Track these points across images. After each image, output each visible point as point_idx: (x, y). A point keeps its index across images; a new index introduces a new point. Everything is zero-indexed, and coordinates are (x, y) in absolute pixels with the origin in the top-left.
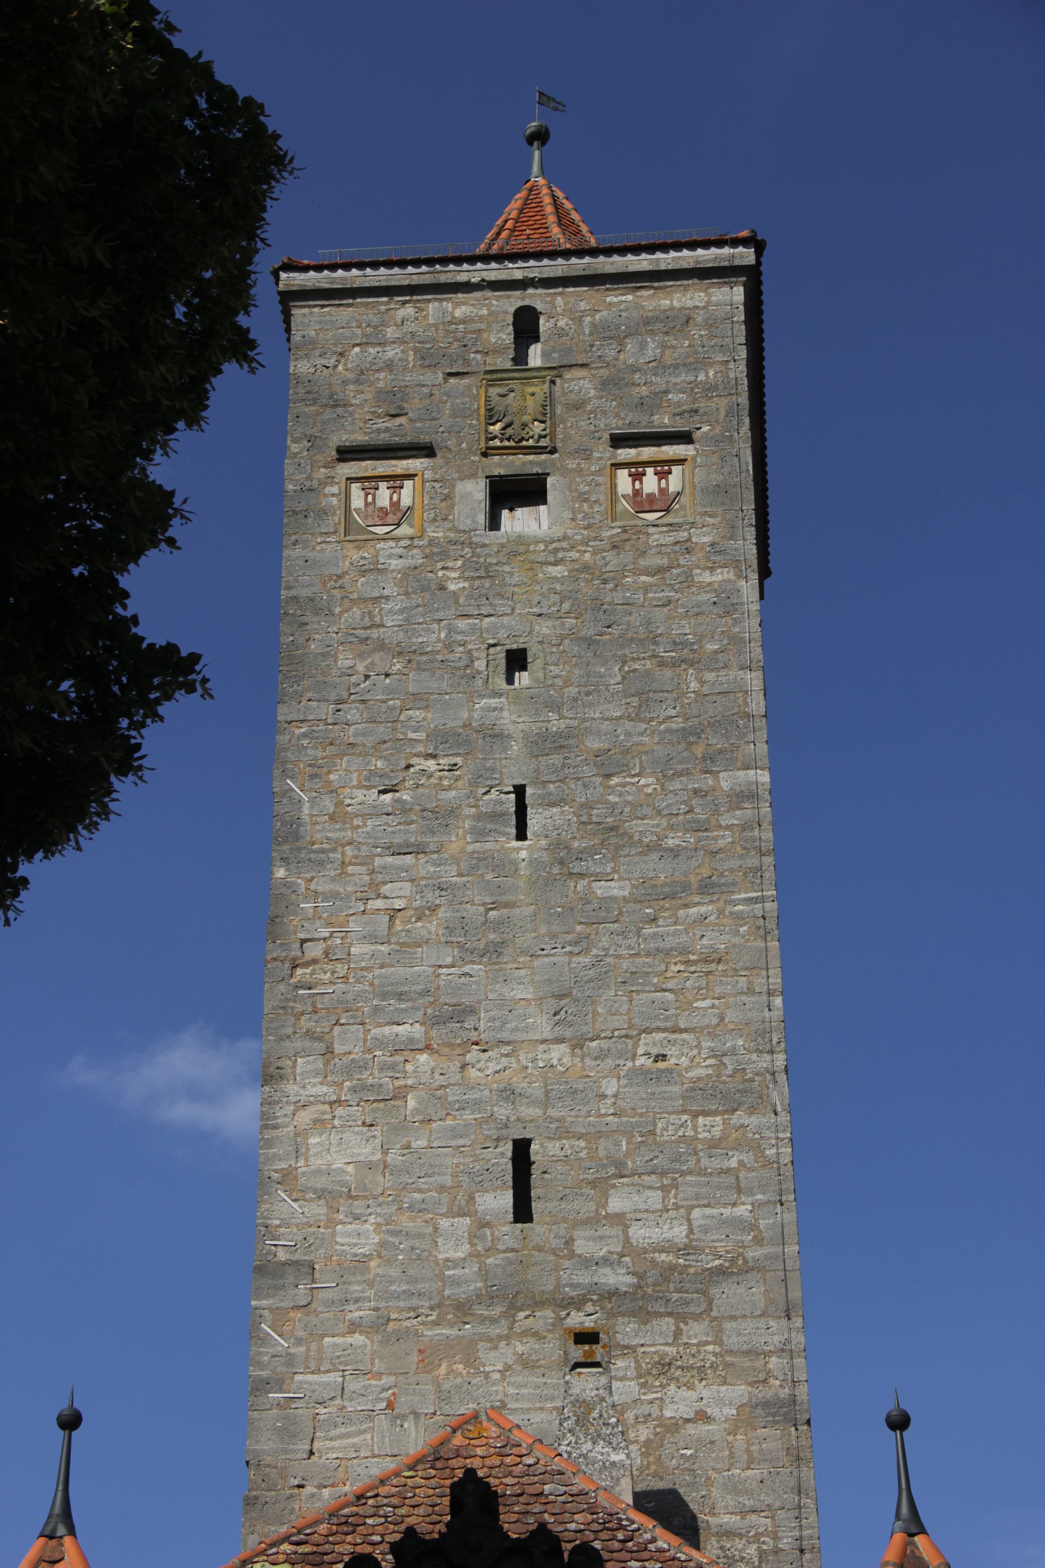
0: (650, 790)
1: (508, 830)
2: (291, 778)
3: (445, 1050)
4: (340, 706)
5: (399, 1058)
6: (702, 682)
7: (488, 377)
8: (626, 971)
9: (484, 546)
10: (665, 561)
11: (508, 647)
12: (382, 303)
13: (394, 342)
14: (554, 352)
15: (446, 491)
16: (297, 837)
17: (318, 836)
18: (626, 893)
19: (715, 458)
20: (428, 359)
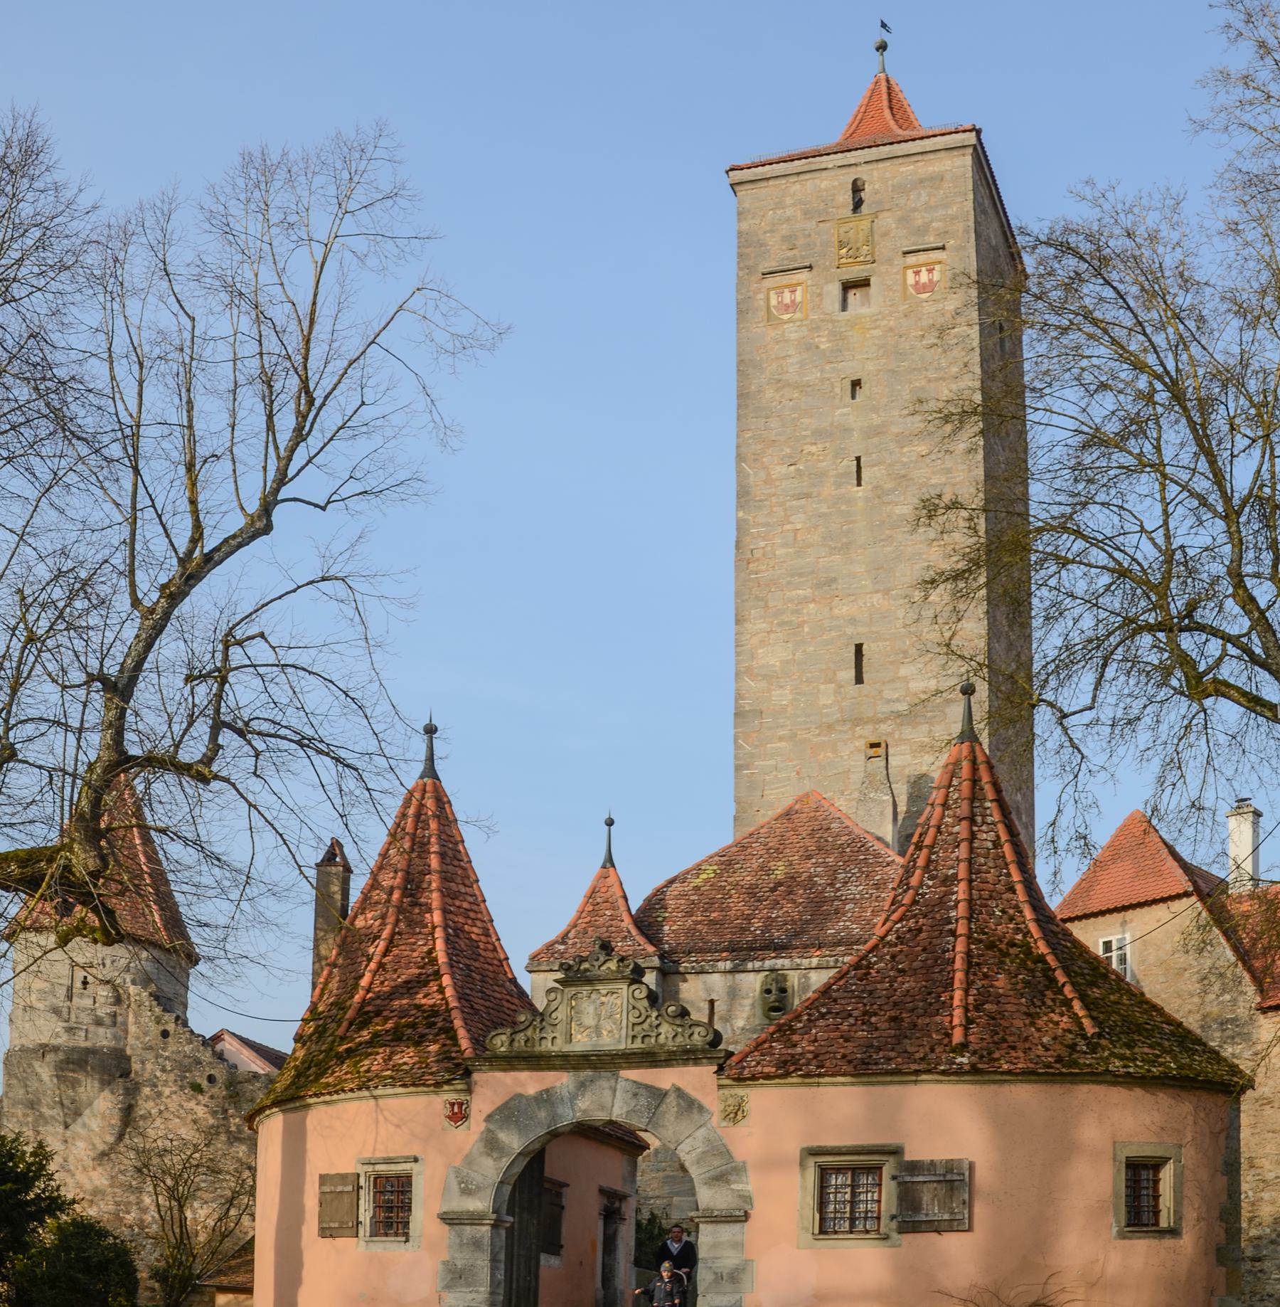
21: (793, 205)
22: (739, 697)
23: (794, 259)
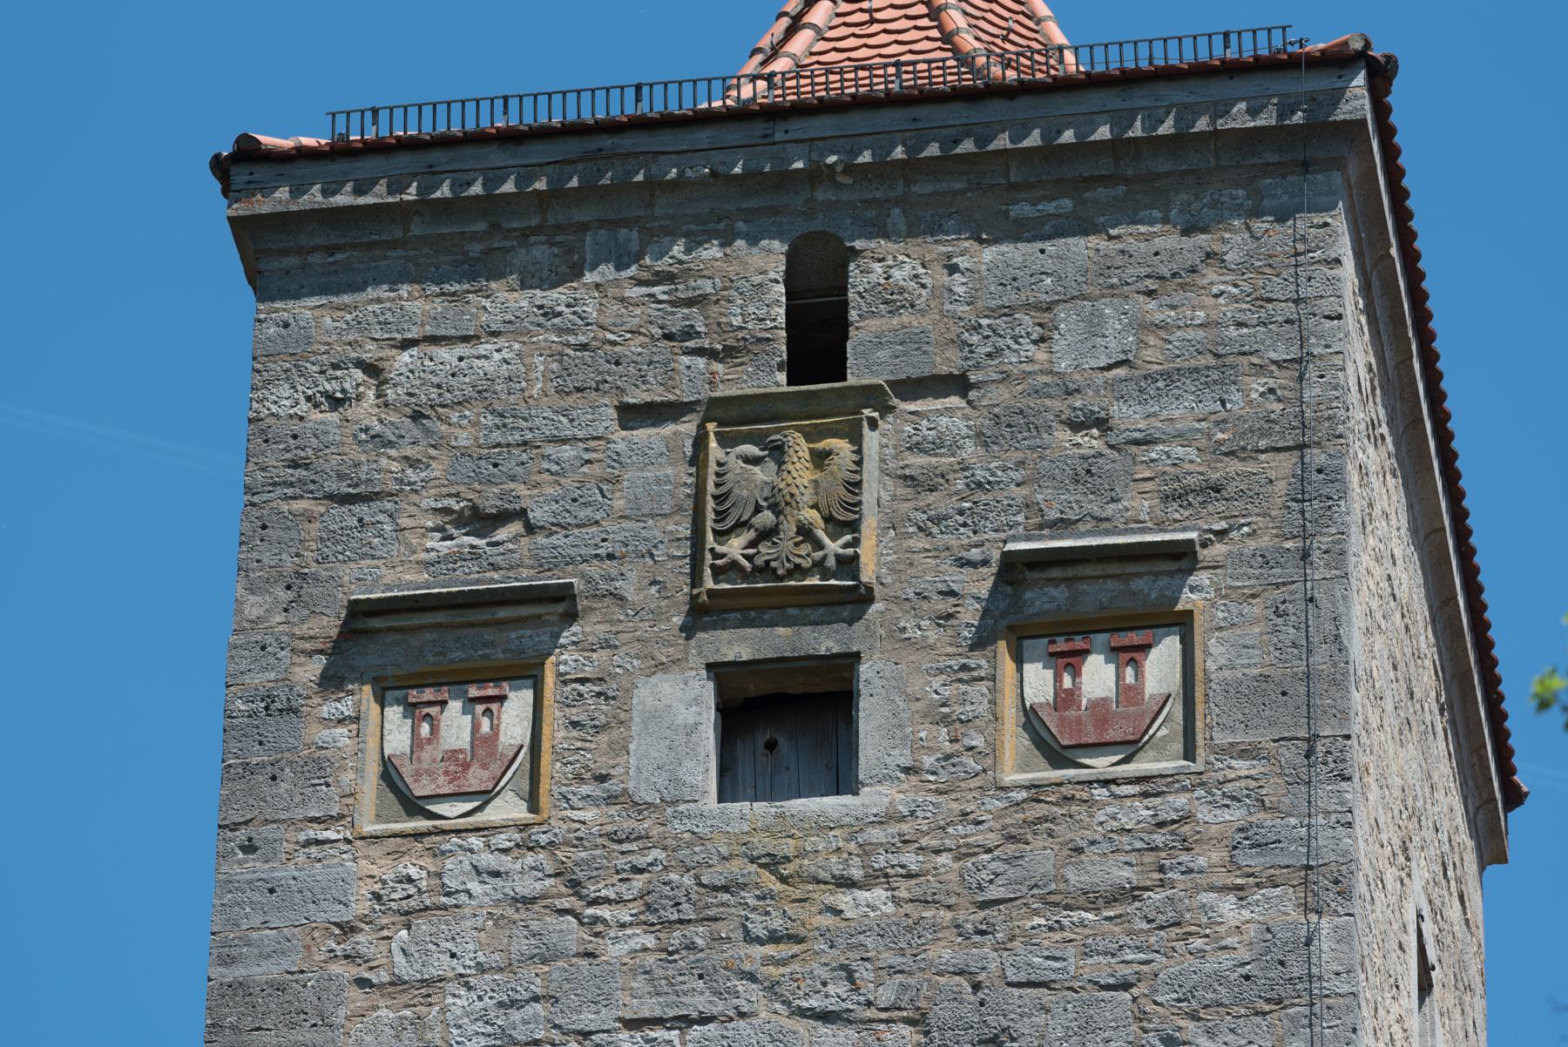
12: (474, 237)
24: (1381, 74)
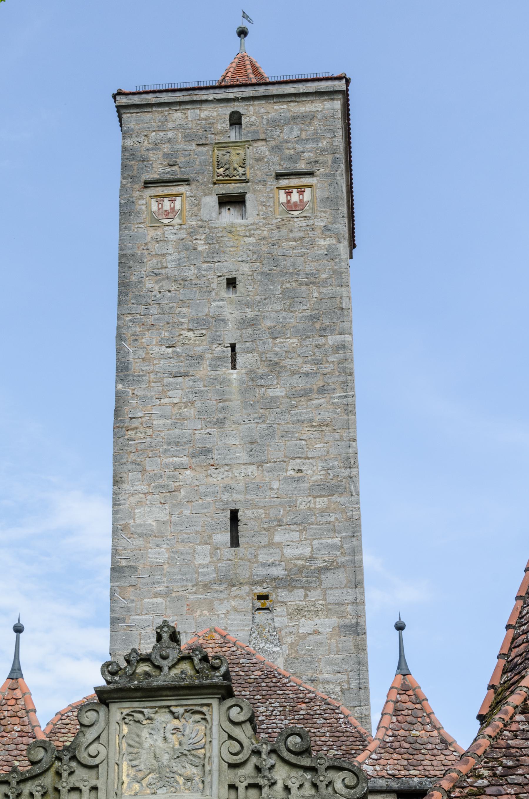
0: (295, 345)
1: (227, 365)
2: (124, 341)
3: (198, 469)
4: (147, 307)
5: (176, 472)
6: (320, 293)
7: (217, 146)
8: (283, 431)
9: (216, 228)
10: (301, 235)
11: (227, 277)
12: (166, 111)
13: (171, 130)
14: (249, 133)
15: (196, 202)
16: (127, 369)
17: (137, 369)
18: (283, 394)
19: (326, 185)
20: (187, 138)
21: (175, 129)
22: (115, 552)
23: (174, 173)
24: (348, 82)
